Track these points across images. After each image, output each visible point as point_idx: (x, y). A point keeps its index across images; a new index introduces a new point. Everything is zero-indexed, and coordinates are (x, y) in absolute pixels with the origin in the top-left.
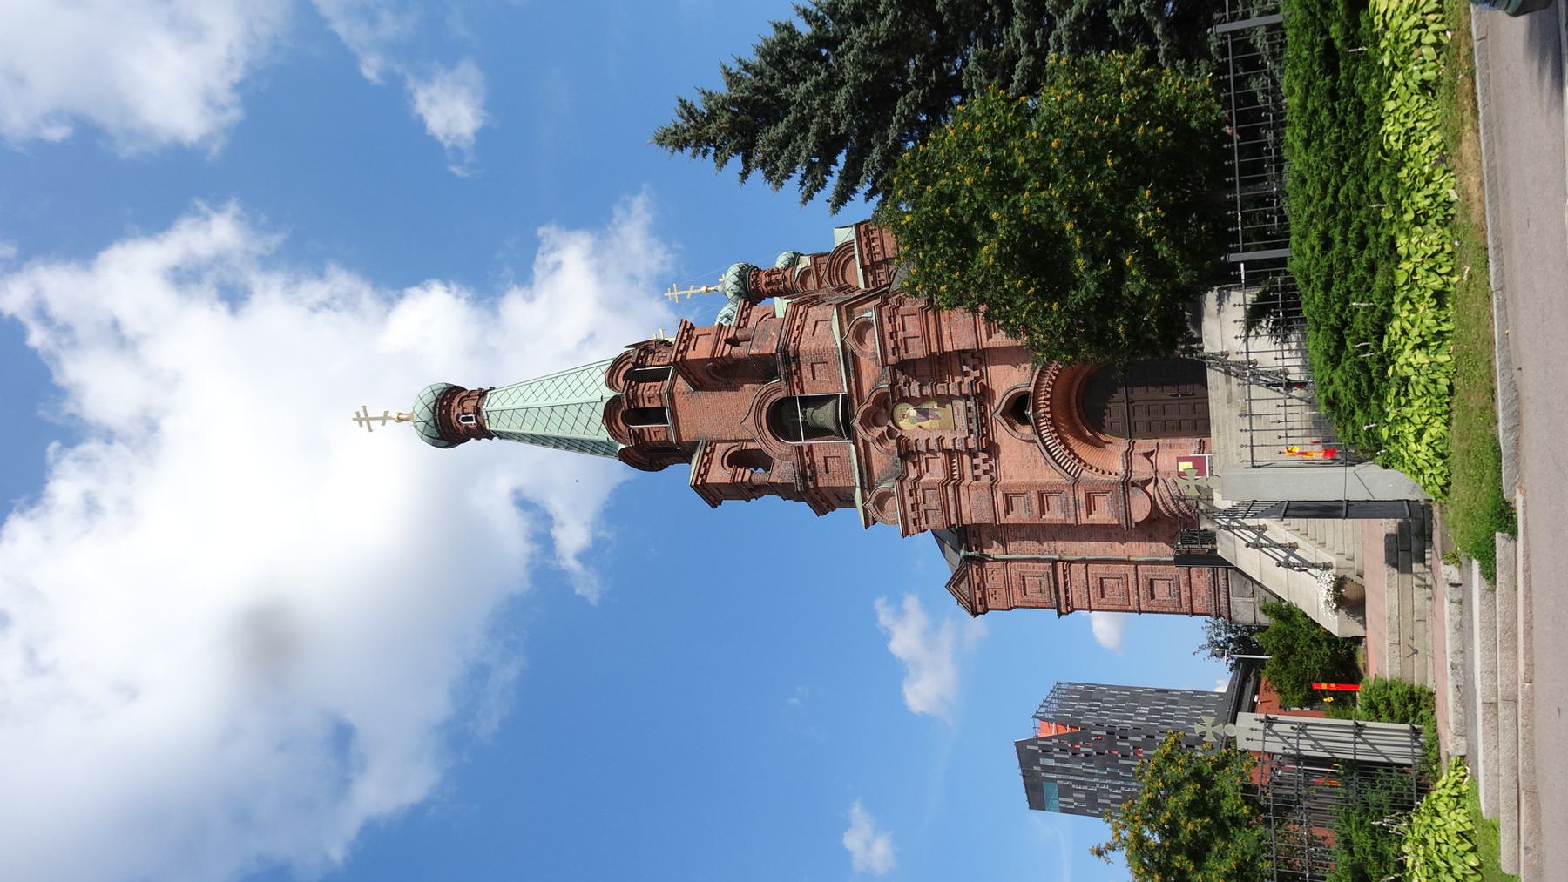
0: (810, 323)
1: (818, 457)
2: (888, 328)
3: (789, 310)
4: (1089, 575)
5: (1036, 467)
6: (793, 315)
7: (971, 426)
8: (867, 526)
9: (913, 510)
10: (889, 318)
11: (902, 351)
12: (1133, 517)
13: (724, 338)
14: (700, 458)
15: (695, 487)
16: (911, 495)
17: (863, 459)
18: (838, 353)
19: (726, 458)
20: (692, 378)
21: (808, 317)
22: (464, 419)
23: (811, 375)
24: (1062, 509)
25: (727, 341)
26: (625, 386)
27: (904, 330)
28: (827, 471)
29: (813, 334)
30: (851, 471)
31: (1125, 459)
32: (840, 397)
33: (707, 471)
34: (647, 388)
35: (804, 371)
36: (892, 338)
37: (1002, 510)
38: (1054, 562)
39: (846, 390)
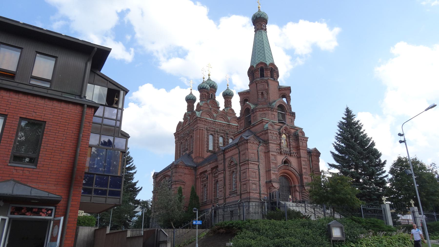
1: (275, 113)
20: (283, 89)
22: (264, 25)
35: (290, 117)
37: (273, 153)
38: (258, 162)
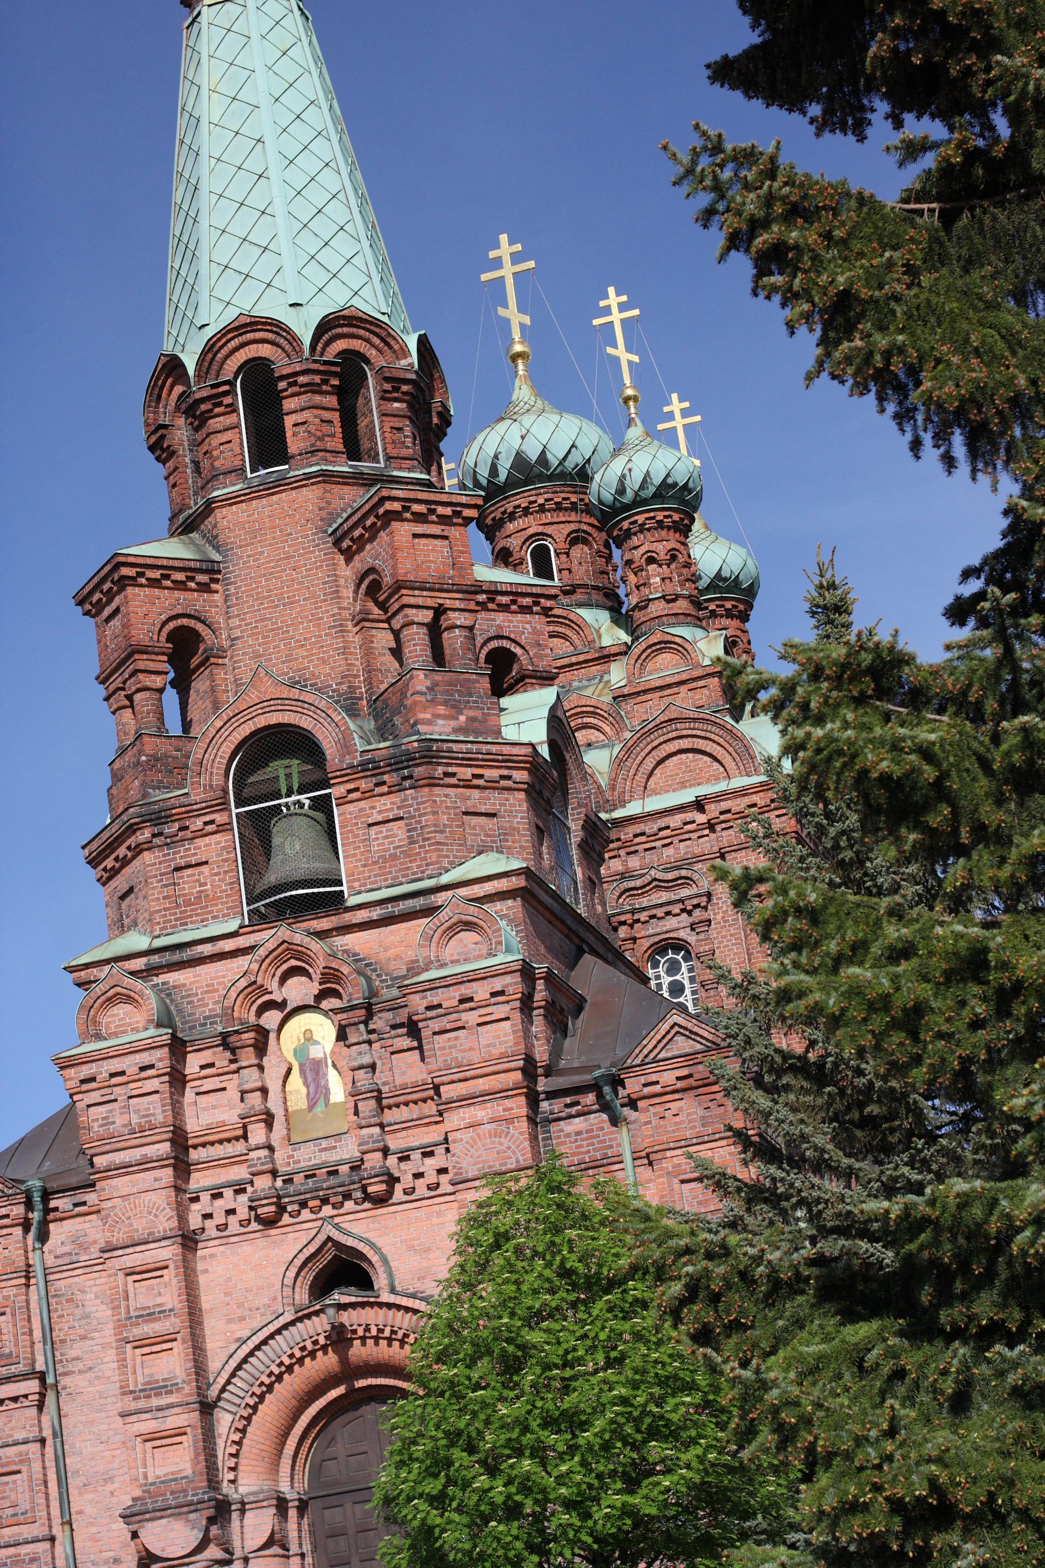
0: (492, 801)
2: (481, 991)
3: (516, 750)
4: (24, 1447)
5: (230, 1321)
6: (508, 761)
7: (298, 1179)
8: (67, 969)
9: (113, 1075)
10: (501, 993)
11: (435, 1024)
12: (149, 1525)
13: (448, 603)
14: (181, 564)
15: (116, 563)
16: (142, 1069)
17: (207, 949)
18: (430, 877)
19: (184, 621)
21: (506, 795)
23: (380, 818)
24: (148, 1383)
25: (439, 611)
26: (326, 363)
27: (479, 1025)
28: (178, 869)
29: (466, 813)
30: (183, 923)
31: (261, 1497)
32: (338, 889)
33: (154, 583)
34: (326, 415)
36: (462, 1001)
39: (352, 901)
